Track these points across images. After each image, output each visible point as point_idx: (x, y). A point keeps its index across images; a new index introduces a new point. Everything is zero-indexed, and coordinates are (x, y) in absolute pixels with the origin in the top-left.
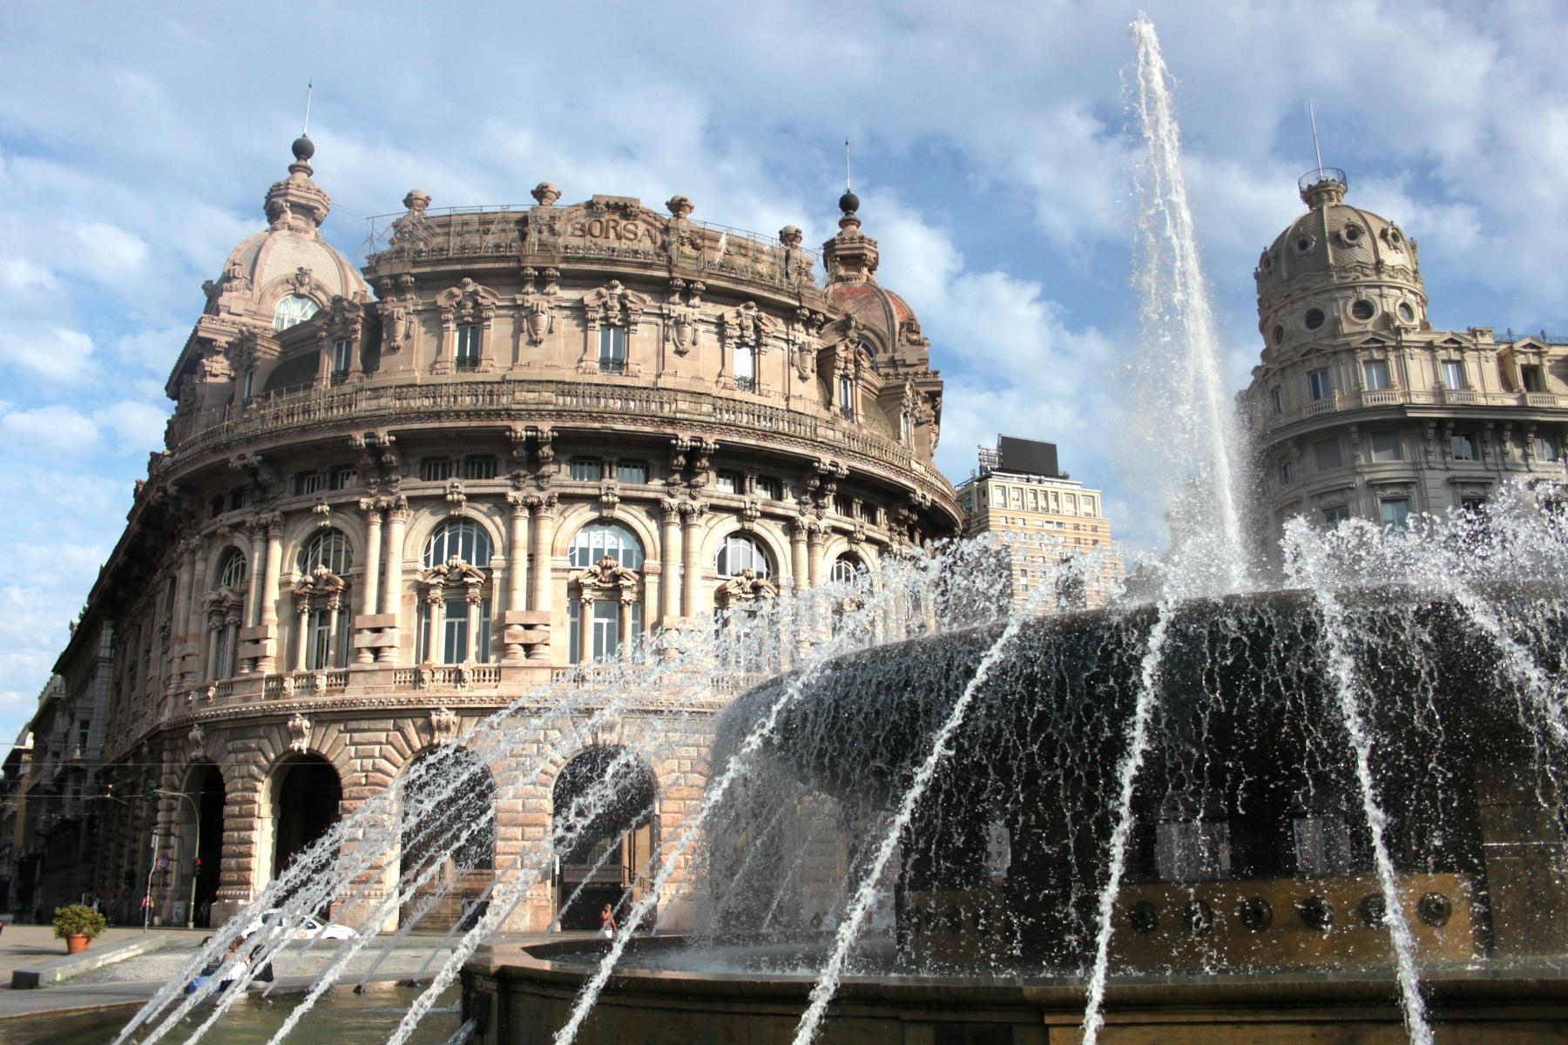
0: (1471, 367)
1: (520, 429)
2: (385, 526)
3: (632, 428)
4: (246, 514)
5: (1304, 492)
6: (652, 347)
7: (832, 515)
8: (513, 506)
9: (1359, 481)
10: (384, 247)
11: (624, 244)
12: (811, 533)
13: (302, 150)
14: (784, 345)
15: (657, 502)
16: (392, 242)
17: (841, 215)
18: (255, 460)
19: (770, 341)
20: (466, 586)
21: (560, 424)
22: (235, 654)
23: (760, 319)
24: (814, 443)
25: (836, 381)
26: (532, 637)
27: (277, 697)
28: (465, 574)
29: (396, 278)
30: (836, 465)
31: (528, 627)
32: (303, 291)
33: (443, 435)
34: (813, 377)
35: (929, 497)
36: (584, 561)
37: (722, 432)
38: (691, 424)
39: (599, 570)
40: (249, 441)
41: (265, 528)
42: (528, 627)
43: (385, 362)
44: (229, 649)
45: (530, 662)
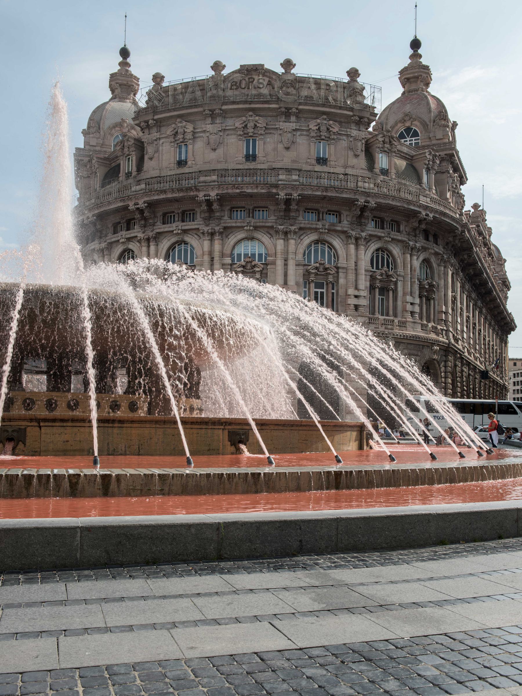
1: (201, 195)
2: (149, 246)
3: (255, 191)
6: (270, 147)
7: (371, 228)
11: (254, 92)
12: (357, 239)
13: (125, 53)
14: (345, 138)
15: (272, 227)
17: (411, 52)
21: (220, 192)
24: (355, 191)
29: (147, 122)
30: (368, 202)
34: (363, 155)
35: (431, 215)
36: (239, 259)
37: (303, 189)
38: (285, 187)
43: (148, 164)
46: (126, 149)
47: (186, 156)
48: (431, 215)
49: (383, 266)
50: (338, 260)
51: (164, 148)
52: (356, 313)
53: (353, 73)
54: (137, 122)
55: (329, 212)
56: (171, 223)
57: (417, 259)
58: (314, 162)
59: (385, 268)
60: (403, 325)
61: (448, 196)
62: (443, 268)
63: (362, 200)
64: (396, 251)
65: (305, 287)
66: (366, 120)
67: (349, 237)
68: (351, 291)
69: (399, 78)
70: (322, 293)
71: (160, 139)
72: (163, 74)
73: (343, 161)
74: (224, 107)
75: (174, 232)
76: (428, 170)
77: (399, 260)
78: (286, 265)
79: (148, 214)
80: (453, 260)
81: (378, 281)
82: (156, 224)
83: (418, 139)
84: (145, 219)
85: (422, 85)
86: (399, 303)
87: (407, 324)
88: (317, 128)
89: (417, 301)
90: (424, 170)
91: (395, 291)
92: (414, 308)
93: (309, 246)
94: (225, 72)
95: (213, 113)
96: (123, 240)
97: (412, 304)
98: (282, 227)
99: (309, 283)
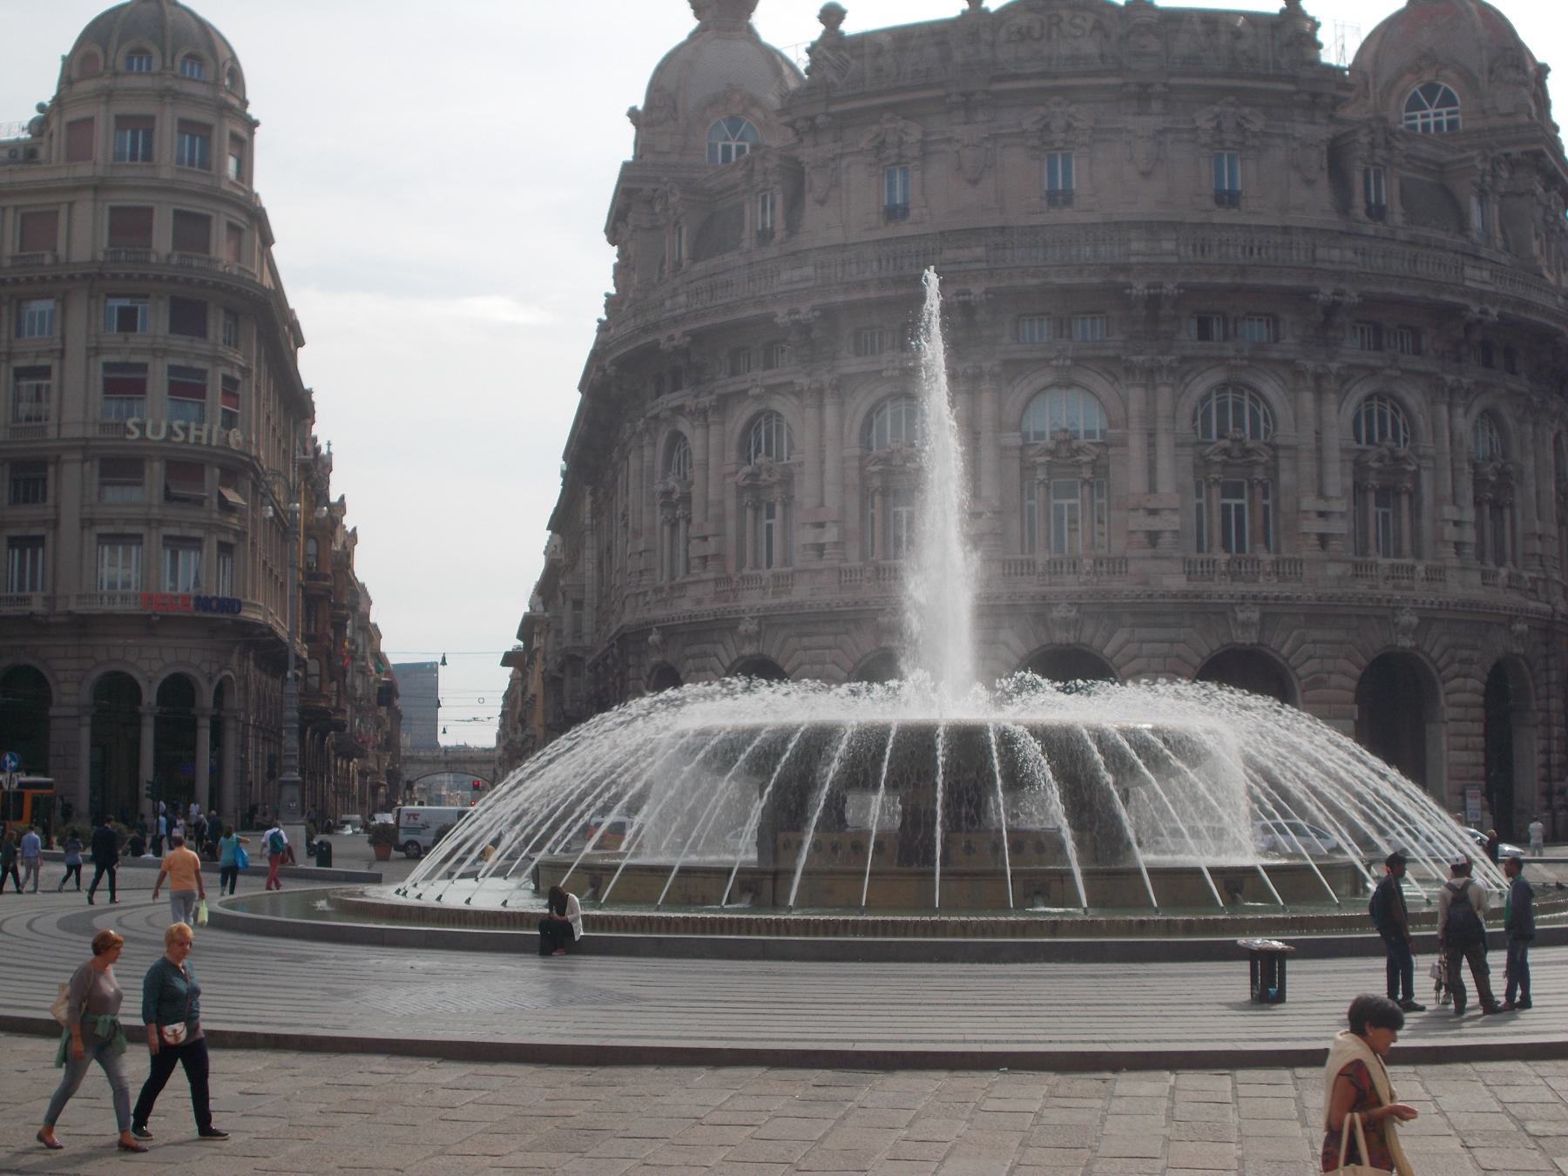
3: (1077, 280)
7: (1352, 350)
12: (1318, 378)
15: (1117, 358)
22: (687, 551)
25: (1358, 177)
27: (727, 601)
29: (812, 119)
34: (1323, 180)
40: (675, 321)
44: (682, 546)
47: (905, 196)
48: (1494, 312)
49: (1383, 434)
50: (1275, 429)
56: (873, 353)
57: (1466, 413)
59: (1389, 443)
60: (1436, 575)
61: (1536, 251)
62: (1530, 428)
63: (1326, 291)
64: (1414, 398)
65: (1199, 495)
67: (1299, 373)
68: (1309, 502)
70: (1239, 508)
71: (842, 156)
72: (844, 5)
74: (997, 87)
76: (1482, 196)
77: (1422, 422)
78: (1152, 446)
86: (1426, 523)
88: (1214, 124)
89: (1469, 514)
90: (1474, 201)
91: (1415, 496)
93: (1205, 399)
96: (756, 391)
97: (1456, 523)
98: (1141, 358)
99: (1209, 487)
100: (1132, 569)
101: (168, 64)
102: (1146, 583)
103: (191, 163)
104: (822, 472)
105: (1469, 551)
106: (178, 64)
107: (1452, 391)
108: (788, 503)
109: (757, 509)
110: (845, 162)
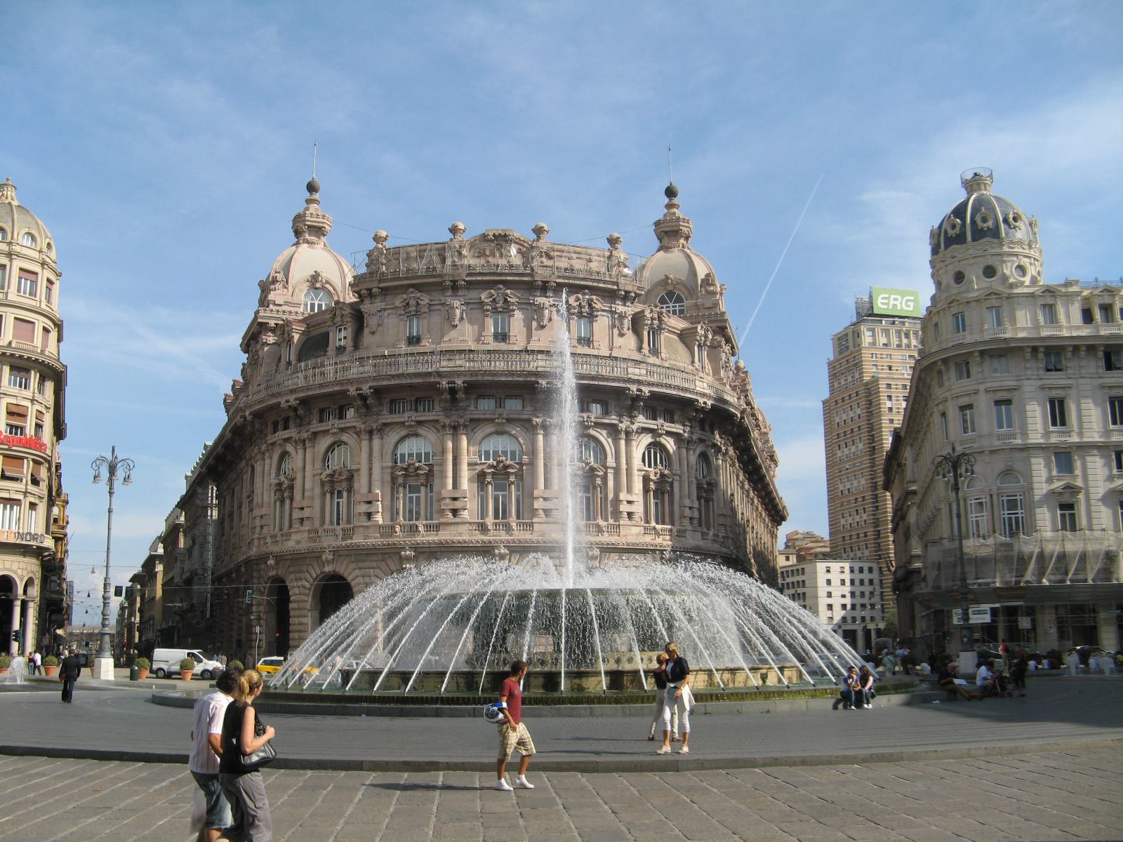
0: (1061, 310)
1: (444, 383)
2: (371, 440)
4: (292, 432)
5: (948, 394)
7: (641, 420)
8: (444, 427)
9: (982, 388)
10: (364, 270)
12: (628, 433)
16: (367, 266)
17: (666, 200)
18: (293, 403)
19: (599, 313)
20: (418, 475)
21: (468, 379)
22: (291, 515)
23: (592, 300)
25: (645, 333)
26: (458, 505)
27: (315, 541)
28: (418, 468)
29: (370, 290)
30: (639, 390)
31: (455, 499)
32: (318, 285)
33: (401, 388)
39: (495, 463)
40: (292, 391)
41: (304, 441)
42: (455, 499)
43: (367, 339)
45: (456, 520)
46: (338, 319)
47: (418, 332)
49: (656, 464)
51: (390, 320)
52: (629, 523)
53: (613, 242)
54: (356, 289)
55: (595, 401)
58: (575, 343)
66: (633, 295)
69: (654, 230)
73: (607, 342)
75: (406, 424)
76: (699, 346)
79: (373, 401)
80: (731, 451)
81: (652, 483)
82: (381, 413)
83: (683, 306)
84: (367, 406)
85: (682, 241)
86: (676, 508)
87: (687, 532)
89: (696, 504)
90: (696, 348)
91: (671, 493)
92: (693, 512)
94: (465, 237)
95: (454, 283)
97: (690, 508)
100: (535, 528)
101: (15, 237)
102: (543, 535)
103: (25, 293)
104: (370, 475)
105: (695, 522)
106: (20, 237)
107: (688, 442)
108: (349, 491)
109: (332, 494)
110: (386, 313)
